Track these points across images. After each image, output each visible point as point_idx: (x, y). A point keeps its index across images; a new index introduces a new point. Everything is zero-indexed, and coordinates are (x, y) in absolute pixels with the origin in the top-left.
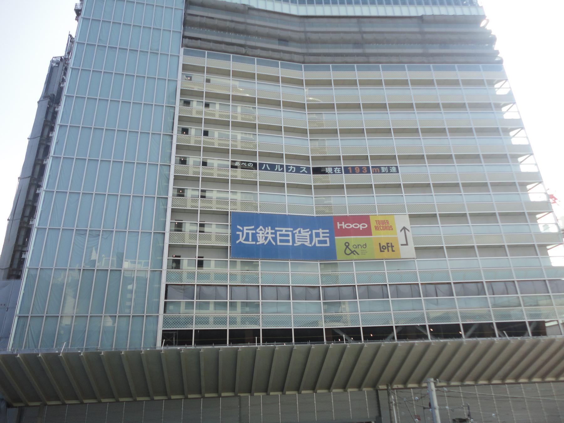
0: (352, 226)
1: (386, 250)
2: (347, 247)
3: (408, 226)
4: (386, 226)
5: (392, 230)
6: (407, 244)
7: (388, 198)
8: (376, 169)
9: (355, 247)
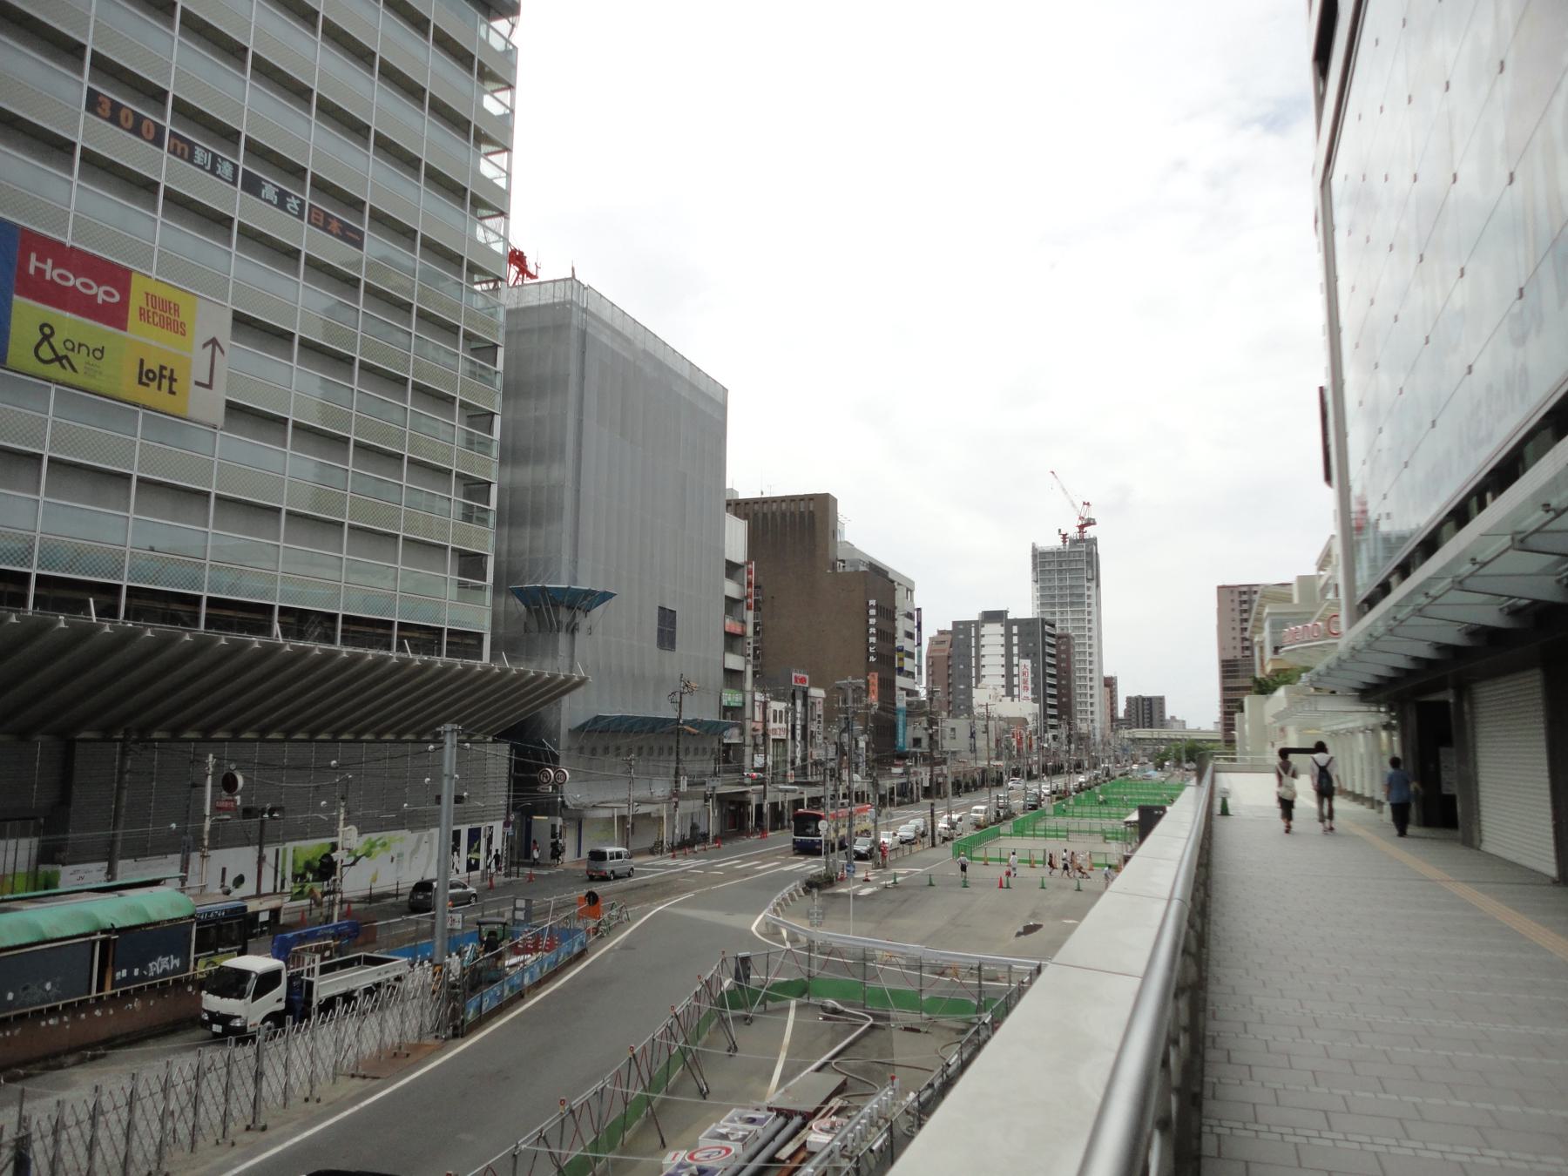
1: (154, 385)
2: (46, 338)
4: (166, 314)
5: (183, 334)
6: (209, 386)
7: (188, 241)
8: (180, 145)
9: (69, 345)
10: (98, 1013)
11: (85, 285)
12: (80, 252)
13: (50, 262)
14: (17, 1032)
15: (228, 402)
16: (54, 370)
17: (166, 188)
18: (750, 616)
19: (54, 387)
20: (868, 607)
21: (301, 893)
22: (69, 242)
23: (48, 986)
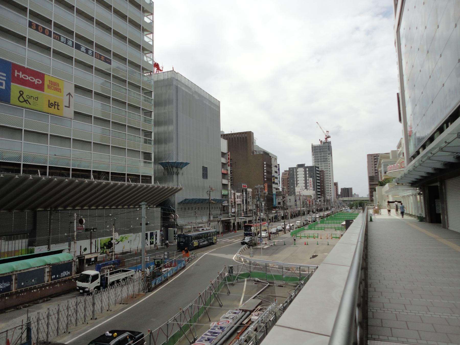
0: (28, 78)
1: (53, 107)
2: (21, 95)
3: (73, 93)
4: (55, 87)
6: (69, 107)
8: (56, 36)
9: (28, 97)
10: (47, 288)
11: (31, 79)
12: (29, 69)
13: (21, 72)
14: (25, 294)
15: (74, 111)
16: (24, 104)
17: (53, 49)
18: (229, 168)
19: (24, 109)
20: (264, 164)
21: (103, 252)
22: (26, 67)
23: (33, 281)
